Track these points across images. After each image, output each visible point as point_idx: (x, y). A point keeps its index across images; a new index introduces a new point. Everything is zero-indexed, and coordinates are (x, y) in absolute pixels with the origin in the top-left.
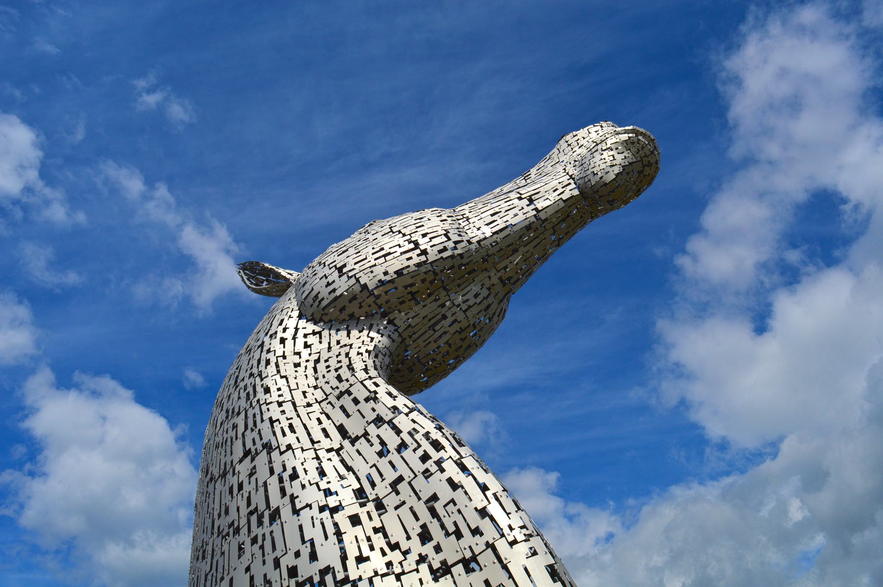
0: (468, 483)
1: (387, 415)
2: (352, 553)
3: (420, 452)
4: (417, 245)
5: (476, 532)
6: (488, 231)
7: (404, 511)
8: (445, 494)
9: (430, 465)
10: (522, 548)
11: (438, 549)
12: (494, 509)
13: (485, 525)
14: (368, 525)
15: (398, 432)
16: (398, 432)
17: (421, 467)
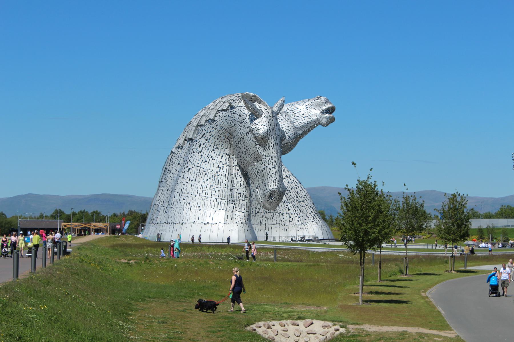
0: (302, 190)
1: (288, 176)
2: (288, 199)
3: (295, 184)
4: (290, 137)
5: (304, 198)
6: (301, 132)
7: (293, 193)
8: (299, 192)
9: (297, 187)
10: (310, 200)
11: (299, 199)
12: (306, 195)
13: (305, 197)
14: (289, 195)
15: (291, 180)
16: (291, 180)
17: (295, 187)
